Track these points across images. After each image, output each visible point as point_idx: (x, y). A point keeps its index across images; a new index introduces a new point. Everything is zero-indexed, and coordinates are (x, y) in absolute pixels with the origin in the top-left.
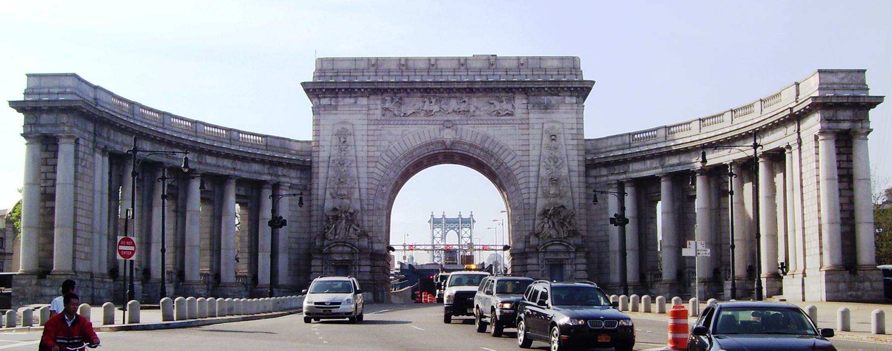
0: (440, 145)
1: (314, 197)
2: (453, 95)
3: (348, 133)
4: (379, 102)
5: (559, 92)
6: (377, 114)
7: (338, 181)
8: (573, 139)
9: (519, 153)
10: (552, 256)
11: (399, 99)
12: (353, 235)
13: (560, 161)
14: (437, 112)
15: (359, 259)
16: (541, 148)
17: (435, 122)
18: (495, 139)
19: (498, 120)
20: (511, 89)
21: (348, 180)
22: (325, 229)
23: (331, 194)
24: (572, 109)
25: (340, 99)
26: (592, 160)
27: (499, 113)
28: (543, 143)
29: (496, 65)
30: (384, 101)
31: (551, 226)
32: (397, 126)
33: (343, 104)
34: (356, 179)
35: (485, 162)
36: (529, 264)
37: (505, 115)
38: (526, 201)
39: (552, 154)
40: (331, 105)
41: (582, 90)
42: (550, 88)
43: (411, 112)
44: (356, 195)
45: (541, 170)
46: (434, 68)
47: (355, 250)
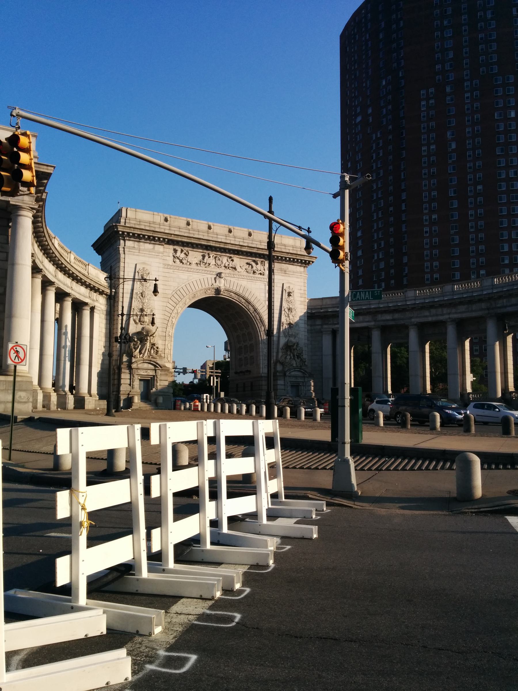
8: (301, 297)
10: (293, 379)
17: (211, 273)
24: (301, 276)
25: (141, 244)
27: (255, 272)
31: (292, 357)
32: (184, 272)
36: (279, 385)
40: (134, 247)
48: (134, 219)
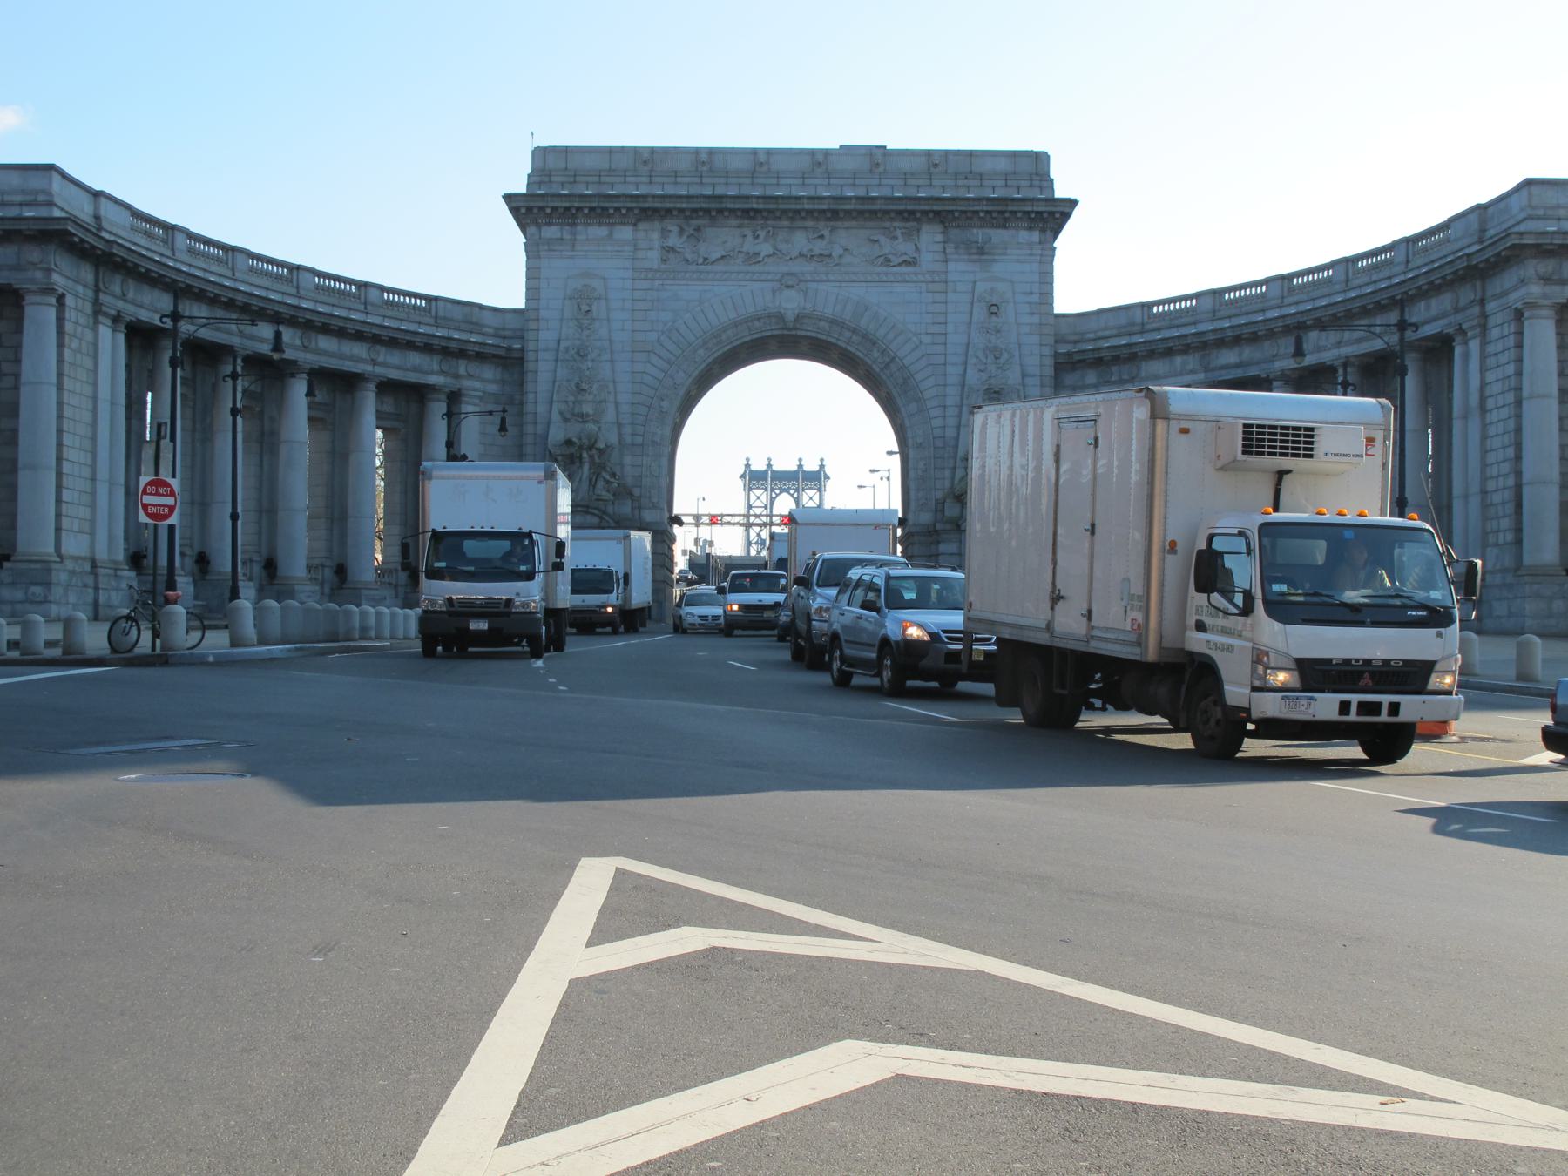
0: (773, 320)
1: (529, 418)
2: (799, 223)
4: (655, 236)
5: (1006, 220)
7: (574, 388)
8: (1032, 314)
9: (927, 339)
11: (695, 230)
12: (604, 493)
13: (1005, 356)
14: (769, 256)
17: (764, 277)
19: (886, 274)
20: (912, 213)
21: (595, 386)
23: (561, 413)
24: (1031, 255)
25: (579, 228)
26: (1069, 354)
27: (889, 260)
28: (975, 319)
30: (665, 233)
32: (690, 283)
33: (584, 237)
34: (611, 386)
35: (861, 356)
36: (943, 554)
37: (900, 265)
38: (938, 432)
39: (990, 342)
40: (562, 239)
41: (1055, 215)
42: (988, 212)
43: (718, 255)
44: (610, 415)
45: (969, 372)
46: (765, 168)
47: (608, 522)
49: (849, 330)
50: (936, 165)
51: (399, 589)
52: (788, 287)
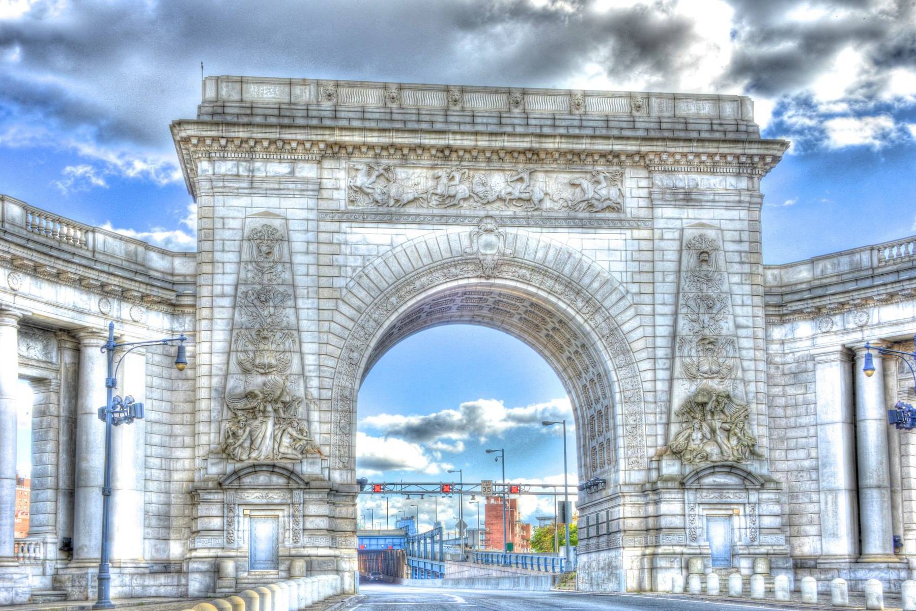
3: (277, 236)
4: (342, 175)
5: (715, 164)
6: (338, 200)
8: (742, 263)
9: (634, 288)
11: (385, 169)
12: (290, 451)
13: (718, 305)
15: (304, 502)
16: (679, 278)
18: (584, 258)
20: (617, 155)
22: (229, 437)
23: (240, 364)
25: (258, 164)
27: (592, 206)
28: (683, 268)
29: (585, 106)
37: (603, 210)
39: (701, 290)
40: (238, 175)
45: (681, 322)
46: (458, 108)
48: (236, 102)
49: (551, 278)
50: (639, 107)
51: (48, 563)
52: (486, 231)
